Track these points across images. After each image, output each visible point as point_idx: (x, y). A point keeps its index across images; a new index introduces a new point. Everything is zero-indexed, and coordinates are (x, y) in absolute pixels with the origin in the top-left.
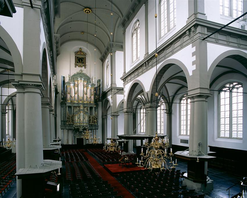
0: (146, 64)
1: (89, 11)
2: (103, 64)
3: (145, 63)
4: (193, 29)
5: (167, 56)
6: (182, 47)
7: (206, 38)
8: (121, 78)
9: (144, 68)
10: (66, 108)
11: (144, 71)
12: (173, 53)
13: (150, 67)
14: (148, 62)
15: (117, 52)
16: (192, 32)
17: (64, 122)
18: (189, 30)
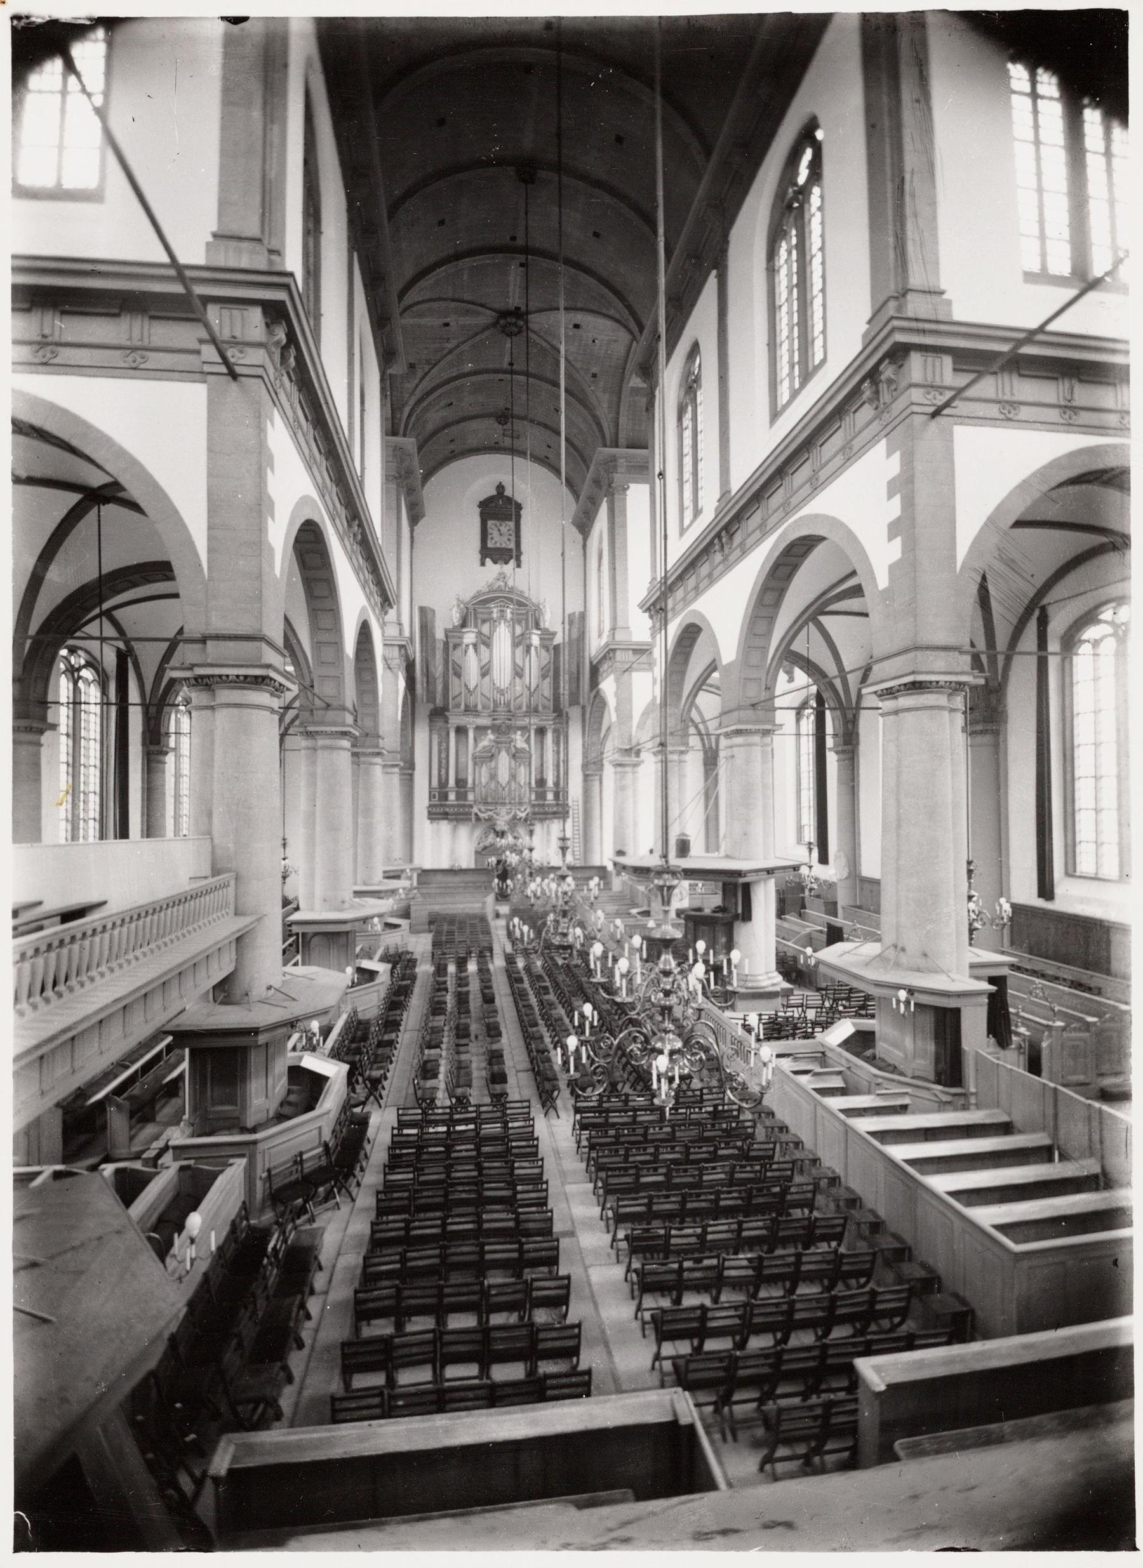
0: (724, 540)
1: (515, 324)
2: (584, 546)
3: (718, 536)
4: (888, 371)
5: (794, 501)
6: (850, 455)
7: (947, 404)
8: (641, 606)
9: (718, 557)
10: (448, 734)
11: (716, 573)
12: (816, 485)
13: (738, 552)
14: (727, 532)
15: (632, 486)
16: (883, 387)
17: (439, 793)
18: (873, 375)
